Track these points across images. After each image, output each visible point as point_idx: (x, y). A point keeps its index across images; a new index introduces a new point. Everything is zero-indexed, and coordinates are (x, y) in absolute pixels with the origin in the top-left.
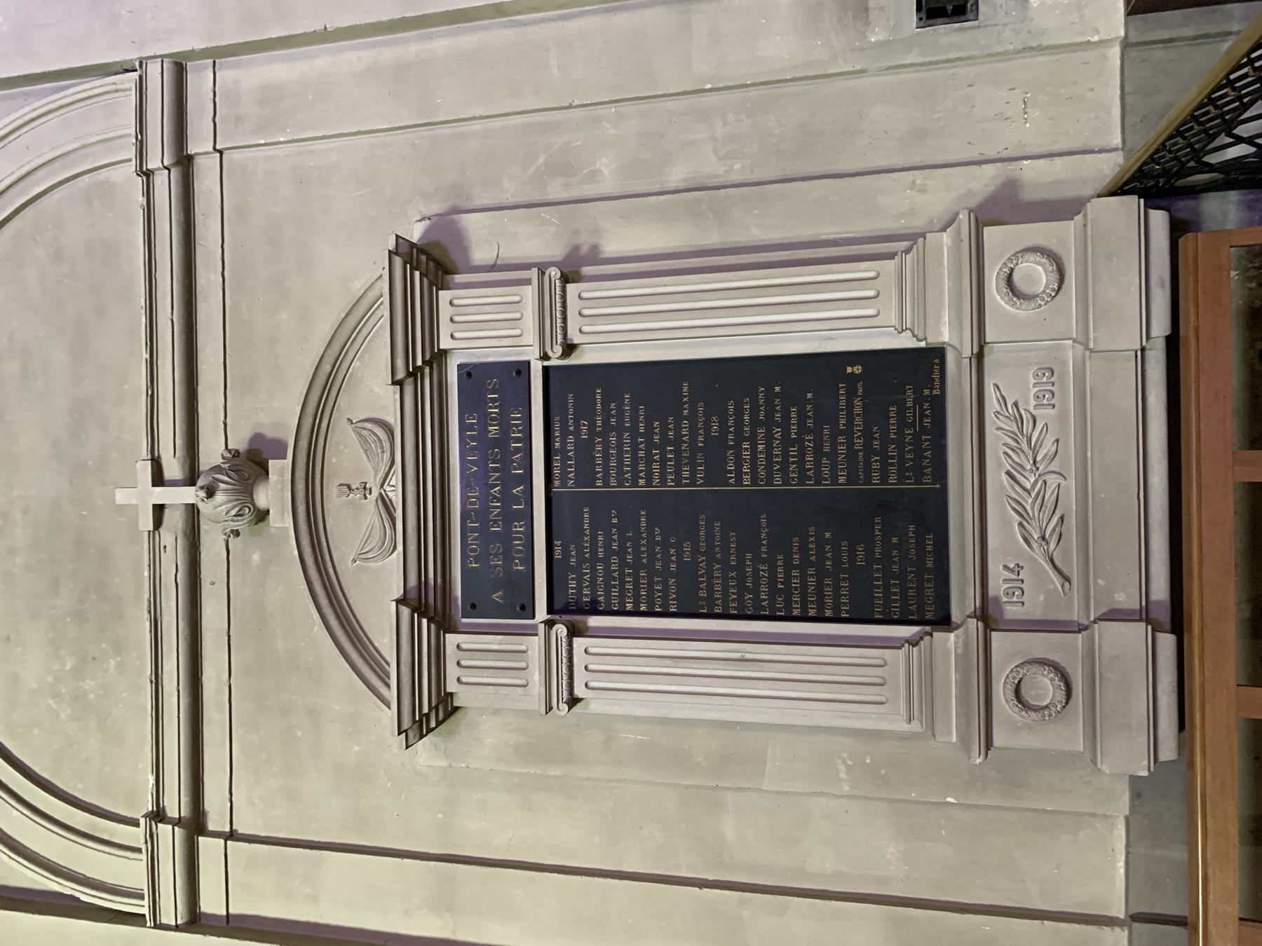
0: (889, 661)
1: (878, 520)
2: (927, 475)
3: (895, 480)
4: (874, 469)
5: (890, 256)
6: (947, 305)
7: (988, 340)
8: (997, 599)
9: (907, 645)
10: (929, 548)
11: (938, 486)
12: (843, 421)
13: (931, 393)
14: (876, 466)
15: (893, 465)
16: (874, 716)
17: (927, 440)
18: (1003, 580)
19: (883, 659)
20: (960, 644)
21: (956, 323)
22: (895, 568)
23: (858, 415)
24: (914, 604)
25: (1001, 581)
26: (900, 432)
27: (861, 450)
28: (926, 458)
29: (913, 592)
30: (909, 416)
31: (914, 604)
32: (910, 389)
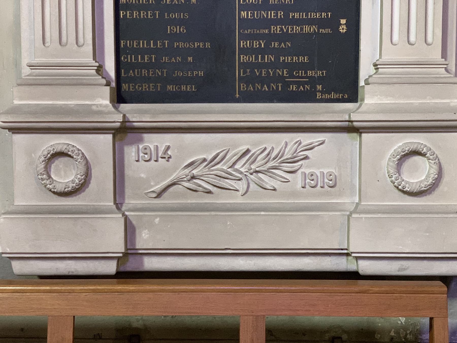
0: (82, 49)
1: (208, 45)
2: (247, 87)
3: (243, 60)
4: (253, 42)
5: (444, 55)
6: (396, 102)
7: (363, 135)
8: (141, 140)
9: (97, 64)
10: (183, 88)
11: (237, 96)
12: (297, 15)
13: (319, 91)
14: (256, 44)
15: (257, 58)
16: (33, 37)
17: (277, 87)
18: (157, 145)
19: (83, 45)
20: (100, 109)
21: (383, 109)
22: (165, 59)
23: (302, 29)
24: (134, 74)
25: (157, 144)
26: (285, 65)
27: (270, 31)
28: (262, 87)
29: (145, 74)
30: (299, 73)
31: (134, 74)
32: (323, 73)
